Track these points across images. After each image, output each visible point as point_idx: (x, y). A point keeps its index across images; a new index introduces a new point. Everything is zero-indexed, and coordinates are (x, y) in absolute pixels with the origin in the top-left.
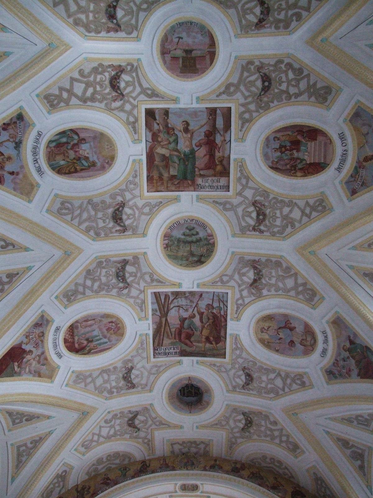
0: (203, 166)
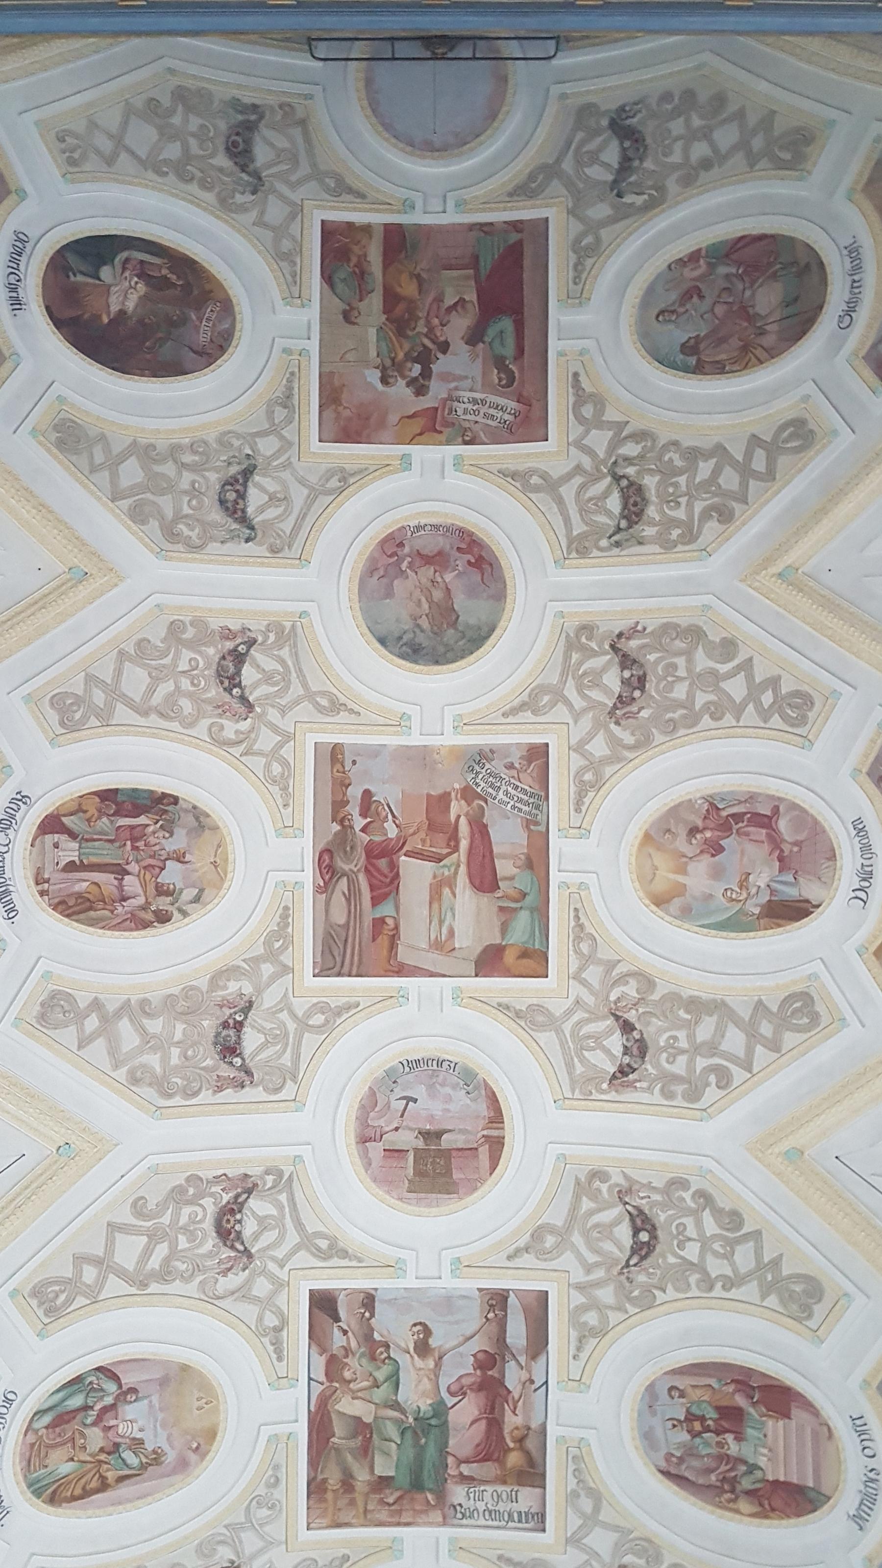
0: (467, 1451)
